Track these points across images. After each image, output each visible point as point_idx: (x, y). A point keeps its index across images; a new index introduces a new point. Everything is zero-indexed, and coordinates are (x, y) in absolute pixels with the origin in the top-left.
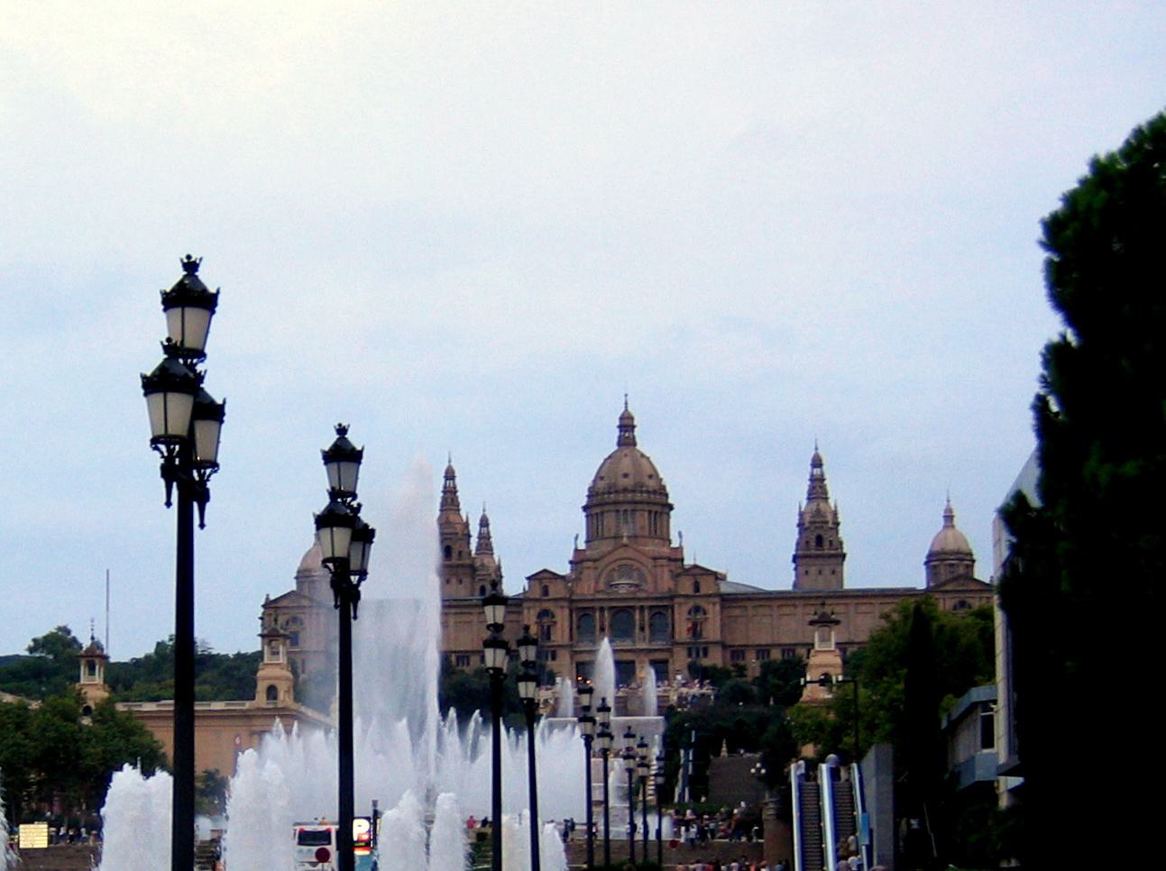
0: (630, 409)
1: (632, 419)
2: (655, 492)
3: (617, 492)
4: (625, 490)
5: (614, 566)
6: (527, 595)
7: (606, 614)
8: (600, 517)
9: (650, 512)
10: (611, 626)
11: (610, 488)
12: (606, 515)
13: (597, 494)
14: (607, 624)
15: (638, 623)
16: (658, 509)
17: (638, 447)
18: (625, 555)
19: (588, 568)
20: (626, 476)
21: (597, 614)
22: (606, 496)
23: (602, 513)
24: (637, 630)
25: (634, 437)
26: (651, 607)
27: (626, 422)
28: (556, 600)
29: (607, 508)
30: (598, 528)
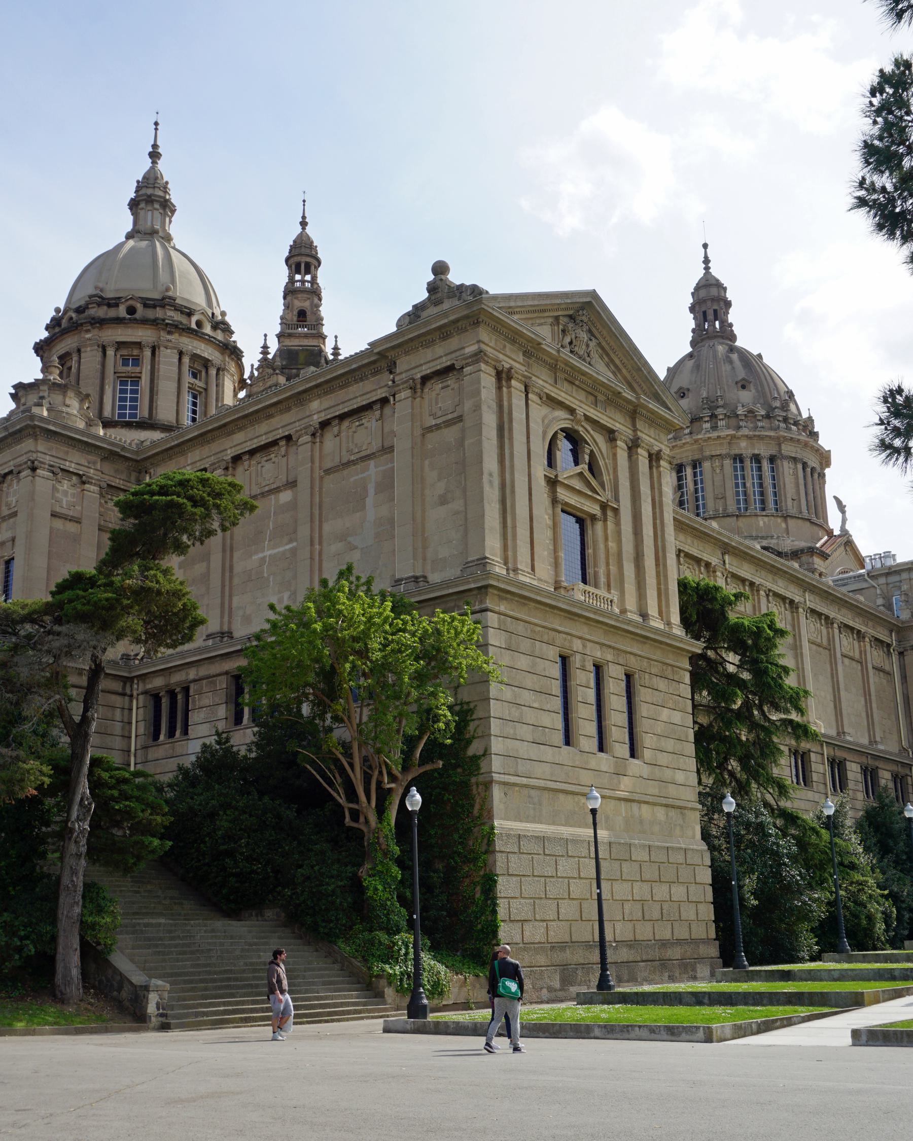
0: (712, 271)
8: (689, 471)
12: (707, 465)
17: (739, 343)
22: (708, 425)
23: (695, 464)
25: (731, 325)
27: (714, 292)
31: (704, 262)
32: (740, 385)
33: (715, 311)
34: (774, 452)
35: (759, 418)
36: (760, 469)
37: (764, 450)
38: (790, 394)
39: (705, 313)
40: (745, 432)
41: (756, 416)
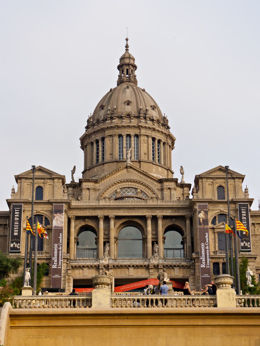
1: (134, 60)
2: (158, 121)
3: (121, 117)
4: (129, 116)
5: (117, 187)
6: (17, 198)
7: (112, 222)
8: (100, 143)
9: (154, 139)
10: (116, 239)
11: (112, 114)
13: (98, 122)
14: (113, 234)
15: (150, 237)
16: (163, 139)
18: (128, 178)
19: (88, 189)
20: (128, 103)
21: (101, 223)
22: (109, 121)
23: (103, 139)
24: (150, 245)
25: (135, 76)
26: (165, 217)
27: (127, 61)
28: (49, 203)
29: (107, 133)
30: (98, 157)
31: (126, 47)
32: (126, 104)
33: (127, 70)
34: (137, 133)
35: (132, 118)
36: (130, 141)
37: (132, 132)
38: (154, 107)
39: (123, 71)
40: (124, 124)
41: (130, 117)
